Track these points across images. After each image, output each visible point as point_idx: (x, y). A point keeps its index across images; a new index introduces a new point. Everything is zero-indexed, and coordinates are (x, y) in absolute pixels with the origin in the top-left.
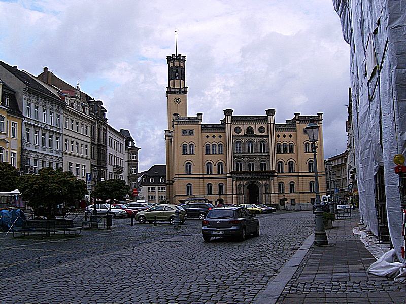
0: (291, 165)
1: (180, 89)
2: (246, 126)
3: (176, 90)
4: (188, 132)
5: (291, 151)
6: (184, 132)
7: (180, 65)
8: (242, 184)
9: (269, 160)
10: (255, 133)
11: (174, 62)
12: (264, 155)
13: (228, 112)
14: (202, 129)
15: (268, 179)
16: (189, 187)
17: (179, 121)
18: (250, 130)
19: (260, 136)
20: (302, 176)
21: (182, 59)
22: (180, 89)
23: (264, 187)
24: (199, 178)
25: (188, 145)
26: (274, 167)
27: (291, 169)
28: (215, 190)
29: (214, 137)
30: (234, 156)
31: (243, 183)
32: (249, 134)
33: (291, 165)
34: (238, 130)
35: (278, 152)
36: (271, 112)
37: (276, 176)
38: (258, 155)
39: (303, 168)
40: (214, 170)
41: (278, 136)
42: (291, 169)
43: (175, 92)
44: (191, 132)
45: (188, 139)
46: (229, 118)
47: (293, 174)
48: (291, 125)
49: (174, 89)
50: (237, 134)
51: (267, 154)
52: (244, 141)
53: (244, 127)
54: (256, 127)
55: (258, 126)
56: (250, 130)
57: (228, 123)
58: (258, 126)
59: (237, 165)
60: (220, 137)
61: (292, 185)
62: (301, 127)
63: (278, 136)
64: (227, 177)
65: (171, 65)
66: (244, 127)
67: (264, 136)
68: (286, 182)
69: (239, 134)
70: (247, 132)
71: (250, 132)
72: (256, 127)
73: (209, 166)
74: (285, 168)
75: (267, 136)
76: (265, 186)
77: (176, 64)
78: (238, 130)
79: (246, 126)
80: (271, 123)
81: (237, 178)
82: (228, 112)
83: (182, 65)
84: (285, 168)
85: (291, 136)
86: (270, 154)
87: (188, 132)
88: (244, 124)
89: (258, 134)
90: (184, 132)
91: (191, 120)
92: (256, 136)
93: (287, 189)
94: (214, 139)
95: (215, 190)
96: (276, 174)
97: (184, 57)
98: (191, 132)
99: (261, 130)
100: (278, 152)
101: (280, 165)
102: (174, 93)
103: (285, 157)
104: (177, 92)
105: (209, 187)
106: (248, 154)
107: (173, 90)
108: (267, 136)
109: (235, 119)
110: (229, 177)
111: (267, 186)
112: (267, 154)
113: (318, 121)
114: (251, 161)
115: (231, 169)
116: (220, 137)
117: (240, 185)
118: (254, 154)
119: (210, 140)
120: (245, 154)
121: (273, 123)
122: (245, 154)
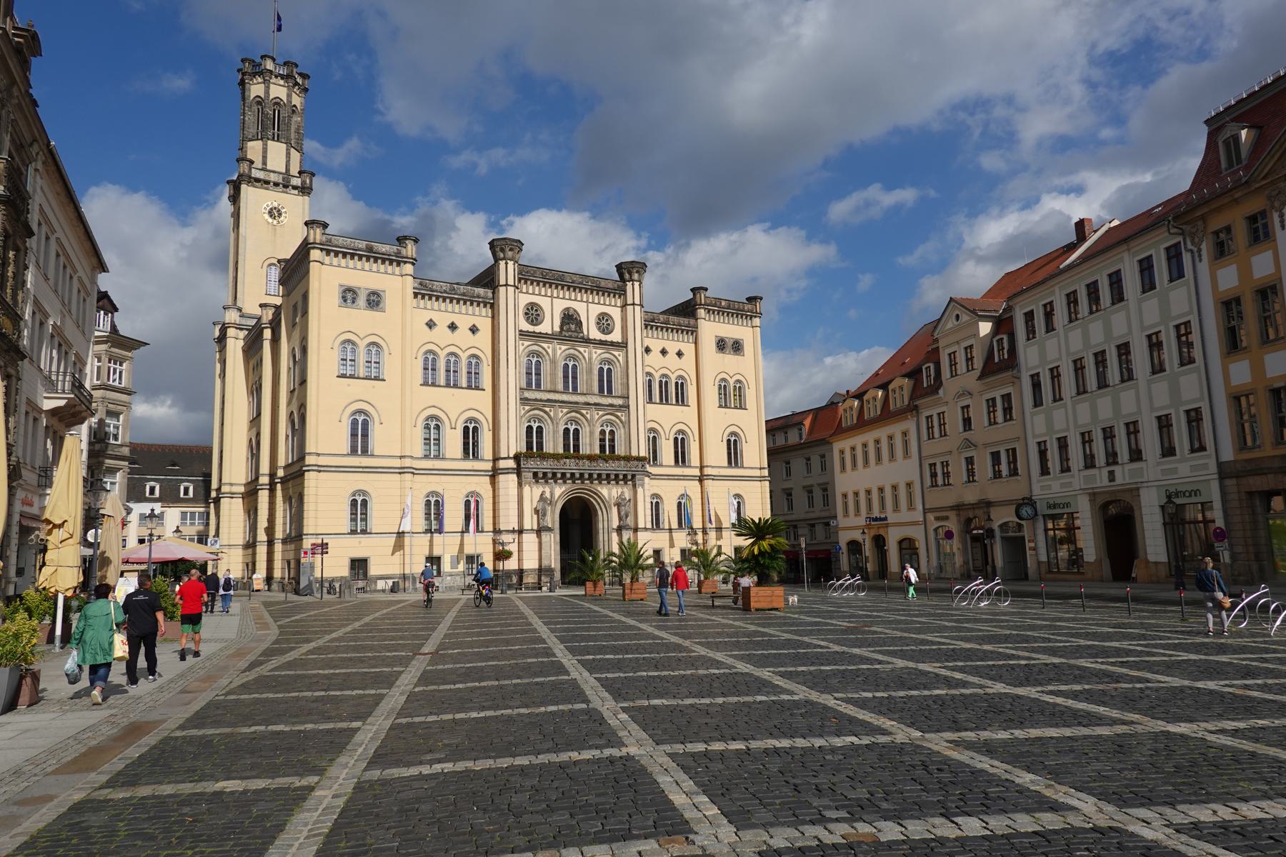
3: (273, 177)
4: (362, 301)
5: (681, 400)
6: (349, 295)
8: (548, 495)
9: (627, 424)
12: (611, 405)
14: (416, 295)
15: (629, 479)
16: (359, 507)
18: (570, 318)
19: (602, 343)
23: (615, 510)
24: (402, 471)
25: (362, 345)
27: (681, 457)
28: (453, 517)
30: (524, 401)
31: (552, 494)
34: (533, 313)
37: (649, 475)
38: (596, 404)
39: (717, 455)
40: (453, 442)
41: (648, 350)
42: (681, 457)
43: (267, 182)
45: (361, 321)
47: (687, 471)
50: (531, 328)
51: (620, 402)
52: (554, 354)
56: (570, 318)
57: (506, 285)
58: (596, 310)
59: (534, 436)
63: (648, 350)
64: (494, 474)
66: (554, 306)
67: (612, 344)
68: (670, 493)
69: (538, 329)
71: (573, 327)
73: (433, 427)
74: (667, 452)
75: (623, 345)
76: (618, 505)
78: (533, 313)
79: (560, 305)
81: (535, 474)
85: (680, 354)
88: (552, 296)
89: (595, 334)
90: (349, 295)
92: (587, 341)
93: (670, 513)
95: (453, 517)
98: (375, 300)
99: (604, 322)
100: (650, 401)
103: (668, 418)
104: (276, 184)
105: (434, 509)
106: (565, 397)
107: (260, 175)
108: (623, 345)
110: (507, 471)
112: (620, 402)
114: (572, 420)
115: (512, 441)
116: (474, 330)
117: (542, 498)
119: (441, 335)
121: (641, 305)
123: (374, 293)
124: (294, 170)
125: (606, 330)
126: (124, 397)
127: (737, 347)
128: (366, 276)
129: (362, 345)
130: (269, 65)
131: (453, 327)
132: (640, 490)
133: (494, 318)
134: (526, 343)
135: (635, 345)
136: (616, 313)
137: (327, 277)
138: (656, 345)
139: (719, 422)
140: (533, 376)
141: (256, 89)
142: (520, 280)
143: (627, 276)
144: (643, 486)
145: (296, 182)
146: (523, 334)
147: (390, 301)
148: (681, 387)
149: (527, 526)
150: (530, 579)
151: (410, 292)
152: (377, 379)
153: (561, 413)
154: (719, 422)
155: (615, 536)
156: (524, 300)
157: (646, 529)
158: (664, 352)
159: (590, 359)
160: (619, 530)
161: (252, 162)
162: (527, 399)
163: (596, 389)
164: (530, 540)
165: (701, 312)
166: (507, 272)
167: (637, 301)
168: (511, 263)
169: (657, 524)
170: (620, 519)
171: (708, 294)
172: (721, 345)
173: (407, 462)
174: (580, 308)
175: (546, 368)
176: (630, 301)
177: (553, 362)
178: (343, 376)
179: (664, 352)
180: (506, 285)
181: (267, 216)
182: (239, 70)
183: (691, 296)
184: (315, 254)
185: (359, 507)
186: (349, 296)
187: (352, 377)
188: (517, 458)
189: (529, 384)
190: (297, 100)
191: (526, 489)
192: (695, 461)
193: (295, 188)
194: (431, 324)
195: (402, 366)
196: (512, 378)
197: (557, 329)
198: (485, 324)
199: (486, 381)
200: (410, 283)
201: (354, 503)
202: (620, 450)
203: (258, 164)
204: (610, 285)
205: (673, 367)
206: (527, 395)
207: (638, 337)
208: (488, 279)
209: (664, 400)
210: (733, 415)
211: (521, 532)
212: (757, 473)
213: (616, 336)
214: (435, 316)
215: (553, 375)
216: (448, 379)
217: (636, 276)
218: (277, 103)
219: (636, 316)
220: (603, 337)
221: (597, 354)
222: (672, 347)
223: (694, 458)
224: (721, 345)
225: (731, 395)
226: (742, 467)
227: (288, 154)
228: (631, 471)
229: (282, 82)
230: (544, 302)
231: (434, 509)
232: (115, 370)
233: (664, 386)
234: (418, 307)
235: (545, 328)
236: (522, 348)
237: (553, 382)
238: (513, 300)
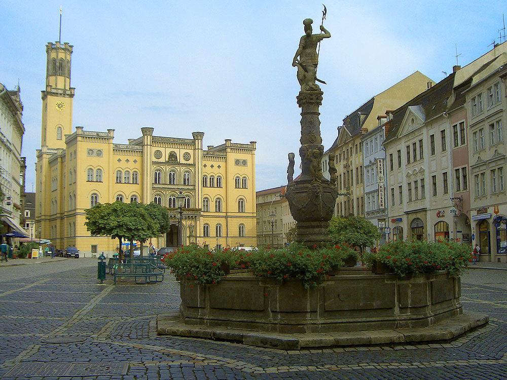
0: (218, 202)
1: (65, 90)
6: (90, 152)
7: (66, 57)
10: (179, 161)
11: (57, 53)
13: (146, 131)
14: (114, 150)
15: (194, 218)
17: (83, 137)
18: (173, 156)
20: (232, 217)
21: (68, 49)
22: (65, 90)
26: (200, 206)
29: (127, 161)
30: (153, 188)
33: (218, 202)
34: (158, 154)
35: (205, 185)
36: (198, 136)
39: (233, 207)
41: (205, 166)
43: (57, 94)
44: (99, 153)
45: (95, 162)
46: (148, 140)
48: (220, 152)
50: (157, 160)
51: (192, 187)
52: (166, 170)
53: (166, 152)
55: (183, 151)
56: (173, 156)
57: (147, 145)
58: (183, 151)
60: (135, 161)
61: (218, 228)
62: (232, 156)
63: (205, 166)
65: (53, 55)
68: (213, 224)
69: (160, 160)
70: (169, 158)
72: (180, 152)
74: (212, 206)
75: (194, 165)
76: (190, 228)
77: (62, 55)
78: (158, 154)
79: (169, 151)
80: (198, 149)
82: (146, 131)
83: (68, 57)
84: (212, 206)
85: (219, 167)
86: (197, 188)
87: (95, 152)
88: (165, 147)
89: (183, 161)
90: (90, 152)
91: (98, 137)
92: (179, 164)
93: (212, 232)
94: (130, 163)
96: (202, 213)
97: (72, 47)
99: (187, 156)
100: (205, 185)
101: (206, 200)
102: (56, 94)
103: (213, 193)
104: (61, 94)
106: (169, 187)
108: (194, 165)
109: (157, 140)
111: (193, 228)
112: (192, 187)
113: (251, 150)
114: (173, 195)
116: (135, 161)
118: (176, 187)
119: (123, 166)
120: (166, 186)
122: (166, 186)
123: (99, 151)
124: (67, 88)
127: (244, 163)
128: (96, 145)
129: (95, 170)
131: (127, 161)
132: (198, 222)
133: (142, 156)
134: (155, 166)
135: (199, 165)
136: (191, 152)
137: (83, 146)
138: (209, 163)
139: (235, 194)
140: (157, 179)
141: (53, 55)
142: (152, 142)
143: (196, 138)
145: (68, 92)
146: (154, 163)
147: (105, 153)
148: (219, 180)
151: (112, 149)
152: (100, 182)
153: (168, 193)
154: (235, 194)
155: (188, 239)
156: (155, 149)
157: (200, 237)
160: (189, 237)
161: (51, 86)
162: (155, 188)
163: (183, 183)
165: (229, 150)
166: (148, 140)
168: (149, 136)
169: (206, 233)
170: (190, 233)
172: (237, 162)
174: (177, 151)
175: (162, 176)
177: (165, 173)
178: (89, 181)
179: (212, 166)
180: (147, 145)
181: (57, 108)
182: (47, 46)
184: (79, 139)
186: (91, 152)
187: (91, 181)
189: (156, 182)
192: (224, 210)
193: (68, 95)
194: (119, 160)
195: (109, 177)
196: (149, 179)
197: (167, 160)
198: (138, 159)
199: (139, 181)
200: (112, 146)
202: (192, 206)
203: (54, 87)
204: (188, 141)
205: (216, 172)
206: (156, 186)
207: (200, 162)
208: (140, 143)
209: (212, 186)
210: (241, 192)
212: (251, 215)
213: (191, 162)
214: (121, 157)
217: (199, 138)
218: (62, 59)
221: (183, 169)
222: (216, 164)
223: (223, 209)
224: (237, 162)
225: (241, 183)
226: (245, 212)
227: (65, 81)
228: (195, 214)
229: (63, 51)
230: (162, 150)
233: (212, 179)
234: (115, 154)
235: (162, 160)
237: (165, 181)
238: (150, 151)
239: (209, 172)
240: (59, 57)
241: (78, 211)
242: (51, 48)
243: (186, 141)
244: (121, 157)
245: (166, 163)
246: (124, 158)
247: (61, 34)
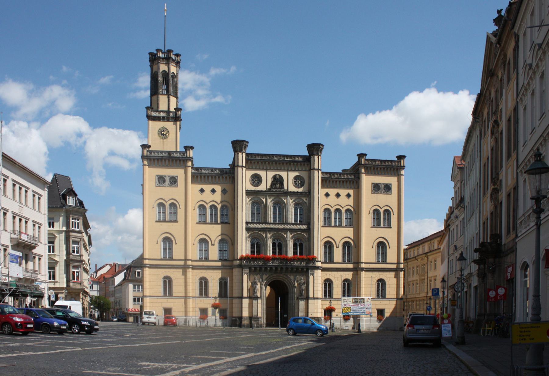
2: (271, 174)
10: (286, 188)
16: (168, 282)
19: (294, 194)
30: (248, 229)
32: (276, 188)
40: (214, 253)
41: (327, 195)
49: (157, 111)
53: (267, 176)
54: (289, 178)
64: (232, 267)
66: (267, 176)
70: (271, 185)
71: (278, 186)
72: (289, 178)
75: (309, 194)
77: (163, 67)
81: (250, 269)
89: (292, 188)
92: (287, 194)
95: (214, 289)
97: (177, 55)
99: (299, 181)
100: (327, 223)
113: (397, 169)
120: (267, 226)
122: (267, 226)
125: (296, 185)
126: (79, 235)
130: (160, 55)
141: (155, 67)
144: (313, 274)
146: (248, 193)
149: (245, 294)
150: (245, 322)
158: (338, 195)
159: (288, 203)
164: (246, 302)
167: (316, 167)
171: (367, 158)
173: (190, 263)
174: (284, 174)
176: (312, 168)
177: (265, 206)
178: (159, 221)
183: (356, 159)
185: (168, 282)
188: (242, 259)
190: (173, 69)
191: (245, 277)
197: (268, 187)
201: (165, 282)
211: (241, 297)
215: (265, 213)
216: (211, 218)
219: (318, 177)
220: (296, 190)
230: (262, 173)
231: (204, 283)
232: (75, 223)
235: (262, 187)
236: (248, 200)
239: (332, 201)
240: (161, 70)
241: (146, 262)
242: (154, 59)
243: (297, 159)
244: (204, 187)
245: (268, 193)
246: (208, 188)
247: (166, 41)
